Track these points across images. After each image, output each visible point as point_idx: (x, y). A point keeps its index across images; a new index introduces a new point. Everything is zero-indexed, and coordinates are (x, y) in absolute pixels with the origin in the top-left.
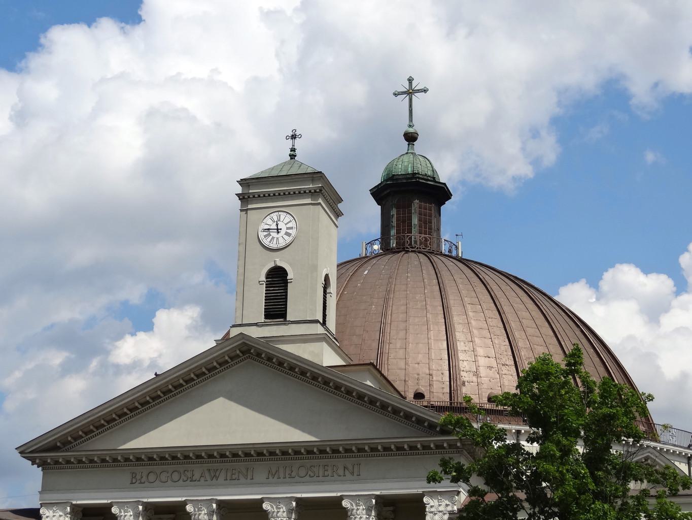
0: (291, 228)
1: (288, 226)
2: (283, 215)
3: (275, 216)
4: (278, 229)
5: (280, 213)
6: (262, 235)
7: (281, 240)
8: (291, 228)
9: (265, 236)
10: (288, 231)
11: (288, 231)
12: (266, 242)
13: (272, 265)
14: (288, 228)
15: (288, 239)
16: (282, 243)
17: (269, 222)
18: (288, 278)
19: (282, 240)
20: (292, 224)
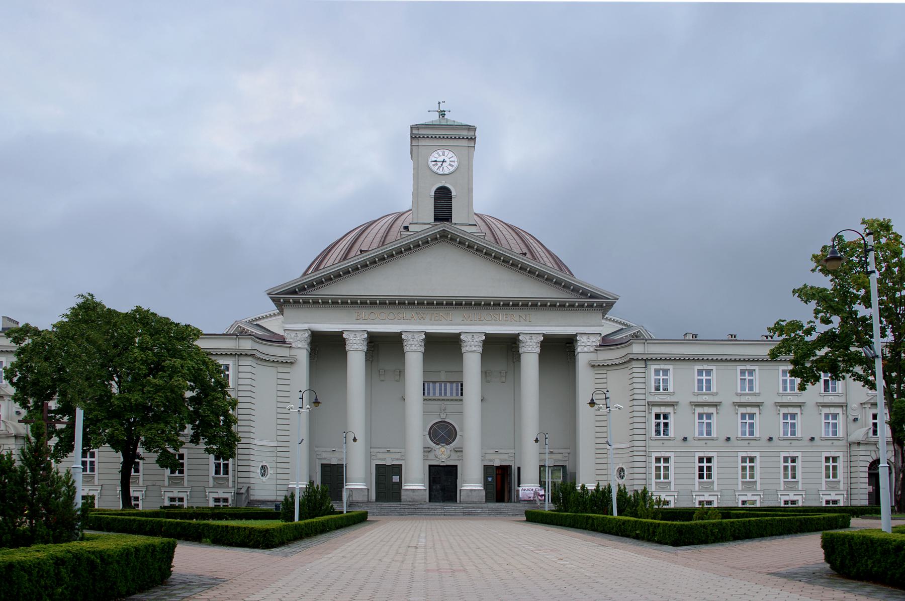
0: (454, 161)
1: (451, 159)
2: (446, 152)
3: (440, 152)
4: (443, 162)
5: (444, 150)
6: (431, 164)
7: (445, 168)
8: (454, 161)
9: (433, 165)
10: (451, 163)
11: (451, 163)
12: (435, 169)
13: (440, 185)
14: (450, 161)
15: (452, 169)
16: (446, 171)
17: (437, 155)
18: (452, 195)
19: (447, 169)
20: (455, 159)
